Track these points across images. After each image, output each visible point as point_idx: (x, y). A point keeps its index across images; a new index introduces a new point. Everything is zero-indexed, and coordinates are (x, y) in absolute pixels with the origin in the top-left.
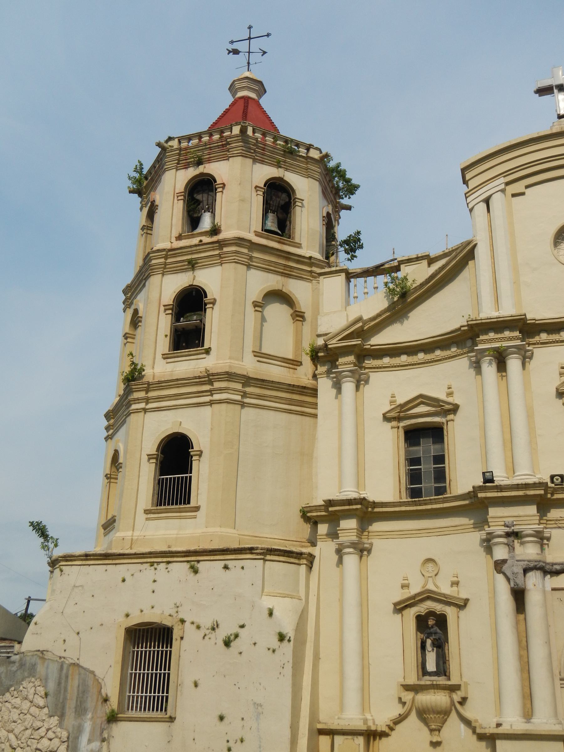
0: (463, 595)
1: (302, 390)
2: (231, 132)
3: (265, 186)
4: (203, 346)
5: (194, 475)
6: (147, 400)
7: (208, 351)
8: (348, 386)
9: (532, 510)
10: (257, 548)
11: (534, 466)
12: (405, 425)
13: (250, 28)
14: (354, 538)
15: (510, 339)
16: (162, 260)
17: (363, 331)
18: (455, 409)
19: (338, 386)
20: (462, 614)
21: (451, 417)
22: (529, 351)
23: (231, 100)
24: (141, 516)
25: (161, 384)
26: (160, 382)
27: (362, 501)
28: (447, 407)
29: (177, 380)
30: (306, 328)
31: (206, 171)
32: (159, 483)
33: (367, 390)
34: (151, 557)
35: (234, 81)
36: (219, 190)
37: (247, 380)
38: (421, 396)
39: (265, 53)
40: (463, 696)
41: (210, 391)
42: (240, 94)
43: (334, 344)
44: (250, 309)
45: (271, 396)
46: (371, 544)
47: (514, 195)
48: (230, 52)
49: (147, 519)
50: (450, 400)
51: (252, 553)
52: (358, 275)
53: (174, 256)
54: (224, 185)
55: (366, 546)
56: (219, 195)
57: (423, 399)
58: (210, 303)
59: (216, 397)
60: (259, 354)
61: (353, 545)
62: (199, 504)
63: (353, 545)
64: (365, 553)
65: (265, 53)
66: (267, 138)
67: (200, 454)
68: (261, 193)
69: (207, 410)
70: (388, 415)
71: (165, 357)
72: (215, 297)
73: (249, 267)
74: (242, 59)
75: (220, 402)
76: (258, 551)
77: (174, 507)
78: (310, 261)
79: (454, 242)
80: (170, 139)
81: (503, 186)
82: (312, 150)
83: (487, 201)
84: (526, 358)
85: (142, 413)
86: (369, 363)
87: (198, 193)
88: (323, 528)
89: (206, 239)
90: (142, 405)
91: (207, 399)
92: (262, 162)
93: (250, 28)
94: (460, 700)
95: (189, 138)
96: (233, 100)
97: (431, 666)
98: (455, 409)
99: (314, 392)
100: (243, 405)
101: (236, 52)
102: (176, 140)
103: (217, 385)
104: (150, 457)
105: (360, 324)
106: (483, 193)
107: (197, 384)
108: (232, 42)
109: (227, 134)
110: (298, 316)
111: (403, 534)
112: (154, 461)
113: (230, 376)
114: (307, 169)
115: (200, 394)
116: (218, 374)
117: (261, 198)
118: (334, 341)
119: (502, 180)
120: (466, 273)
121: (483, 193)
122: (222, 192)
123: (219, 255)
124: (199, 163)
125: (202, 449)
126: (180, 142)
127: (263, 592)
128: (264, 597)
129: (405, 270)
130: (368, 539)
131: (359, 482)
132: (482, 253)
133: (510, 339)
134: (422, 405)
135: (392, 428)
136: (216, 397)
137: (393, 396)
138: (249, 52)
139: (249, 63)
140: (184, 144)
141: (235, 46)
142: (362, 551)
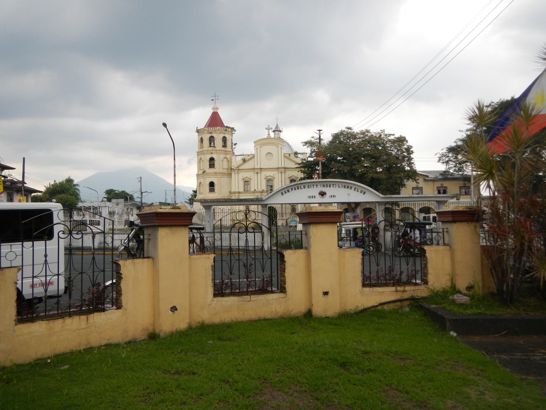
1: (229, 174)
8: (237, 175)
9: (260, 194)
11: (261, 188)
19: (235, 174)
25: (208, 174)
30: (229, 163)
37: (222, 173)
43: (234, 169)
57: (246, 177)
60: (223, 169)
69: (216, 178)
78: (230, 151)
86: (239, 171)
89: (214, 149)
99: (231, 174)
101: (213, 100)
106: (257, 147)
113: (220, 173)
119: (259, 146)
120: (253, 159)
123: (216, 152)
131: (238, 189)
132: (256, 157)
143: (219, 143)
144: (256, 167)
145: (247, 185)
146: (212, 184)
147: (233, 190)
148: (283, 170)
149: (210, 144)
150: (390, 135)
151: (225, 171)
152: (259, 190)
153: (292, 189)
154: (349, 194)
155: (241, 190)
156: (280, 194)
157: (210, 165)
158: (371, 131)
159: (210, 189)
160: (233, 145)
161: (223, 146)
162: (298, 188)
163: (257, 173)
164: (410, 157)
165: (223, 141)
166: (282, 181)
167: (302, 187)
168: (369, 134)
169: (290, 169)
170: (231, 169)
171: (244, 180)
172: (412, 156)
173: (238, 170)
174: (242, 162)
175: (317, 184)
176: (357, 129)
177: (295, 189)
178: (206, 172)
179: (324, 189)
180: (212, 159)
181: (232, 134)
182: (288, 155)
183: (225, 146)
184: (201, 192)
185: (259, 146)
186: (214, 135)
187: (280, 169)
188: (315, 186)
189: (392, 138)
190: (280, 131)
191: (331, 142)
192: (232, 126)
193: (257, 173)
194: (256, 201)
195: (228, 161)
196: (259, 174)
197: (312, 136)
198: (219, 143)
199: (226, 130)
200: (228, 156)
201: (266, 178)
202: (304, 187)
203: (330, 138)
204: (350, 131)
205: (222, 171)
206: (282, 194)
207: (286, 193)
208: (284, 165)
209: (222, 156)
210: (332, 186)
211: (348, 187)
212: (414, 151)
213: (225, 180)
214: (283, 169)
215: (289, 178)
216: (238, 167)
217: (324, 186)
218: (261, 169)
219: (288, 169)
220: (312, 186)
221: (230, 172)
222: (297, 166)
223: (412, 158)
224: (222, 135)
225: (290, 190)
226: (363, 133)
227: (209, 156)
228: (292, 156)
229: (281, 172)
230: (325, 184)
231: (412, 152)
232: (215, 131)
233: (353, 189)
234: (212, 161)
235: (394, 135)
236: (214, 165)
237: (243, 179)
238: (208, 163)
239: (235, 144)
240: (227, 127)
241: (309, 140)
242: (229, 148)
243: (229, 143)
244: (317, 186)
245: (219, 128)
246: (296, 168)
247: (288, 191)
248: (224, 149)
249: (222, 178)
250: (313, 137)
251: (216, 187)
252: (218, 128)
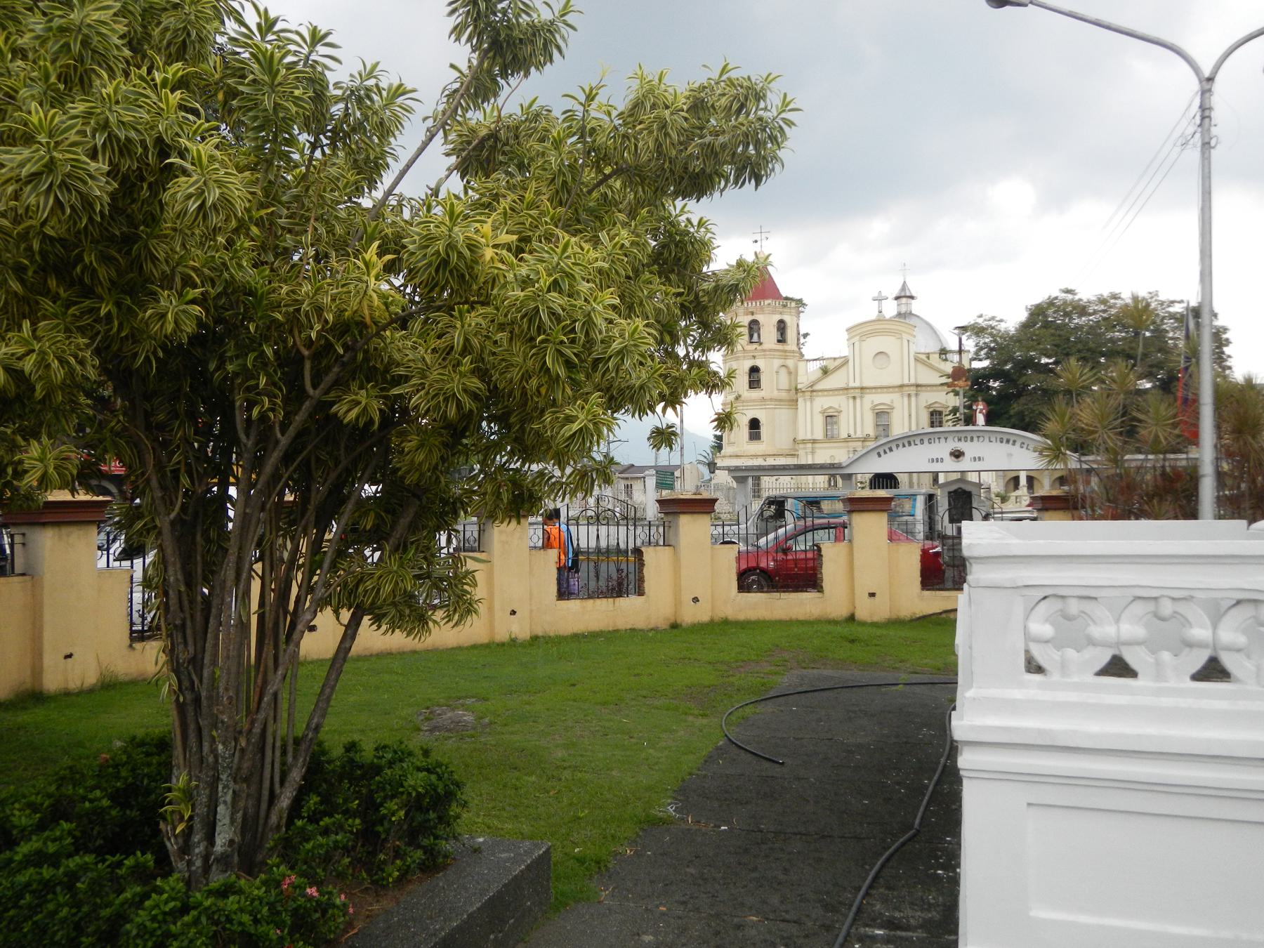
8: (808, 403)
9: (860, 443)
11: (862, 432)
25: (747, 401)
30: (793, 376)
33: (814, 403)
37: (776, 400)
52: (809, 361)
57: (830, 408)
78: (793, 352)
89: (759, 348)
101: (756, 241)
106: (852, 341)
111: (825, 448)
113: (771, 400)
119: (858, 338)
120: (845, 367)
131: (812, 434)
132: (851, 363)
143: (769, 334)
144: (852, 384)
145: (832, 424)
146: (755, 424)
147: (801, 437)
148: (912, 391)
149: (751, 336)
150: (1173, 302)
151: (784, 395)
152: (859, 434)
153: (898, 446)
154: (1010, 455)
155: (819, 434)
156: (875, 454)
157: (750, 382)
158: (1122, 296)
159: (750, 433)
160: (802, 338)
161: (779, 341)
162: (910, 444)
163: (854, 398)
164: (1223, 353)
165: (778, 330)
166: (910, 415)
167: (918, 442)
168: (1119, 302)
170: (797, 390)
172: (1226, 349)
173: (812, 391)
174: (820, 373)
175: (946, 435)
176: (1087, 293)
177: (904, 446)
178: (742, 398)
179: (961, 446)
180: (754, 370)
181: (800, 312)
182: (924, 357)
183: (782, 340)
184: (732, 440)
185: (858, 338)
186: (758, 317)
188: (943, 440)
189: (1177, 308)
190: (912, 297)
191: (1025, 326)
192: (798, 297)
193: (854, 398)
194: (830, 468)
195: (790, 373)
196: (858, 401)
197: (979, 314)
198: (769, 334)
199: (785, 306)
200: (790, 363)
201: (873, 409)
202: (922, 441)
203: (1023, 316)
204: (1070, 297)
205: (776, 394)
206: (879, 455)
207: (885, 452)
208: (916, 378)
209: (777, 363)
210: (975, 439)
211: (1008, 441)
212: (1232, 340)
213: (783, 414)
215: (928, 407)
216: (811, 386)
217: (960, 440)
218: (862, 388)
220: (937, 440)
221: (794, 395)
222: (944, 380)
223: (1229, 356)
224: (778, 317)
225: (894, 448)
226: (1103, 301)
227: (748, 364)
228: (935, 359)
229: (909, 396)
230: (963, 435)
231: (1228, 342)
232: (762, 308)
233: (1018, 444)
234: (755, 375)
235: (1181, 302)
236: (759, 381)
237: (823, 412)
238: (746, 379)
239: (805, 335)
240: (787, 298)
241: (972, 322)
242: (791, 345)
243: (791, 334)
244: (946, 439)
245: (770, 301)
246: (942, 384)
247: (891, 450)
248: (780, 347)
250: (981, 316)
251: (764, 430)
252: (767, 302)
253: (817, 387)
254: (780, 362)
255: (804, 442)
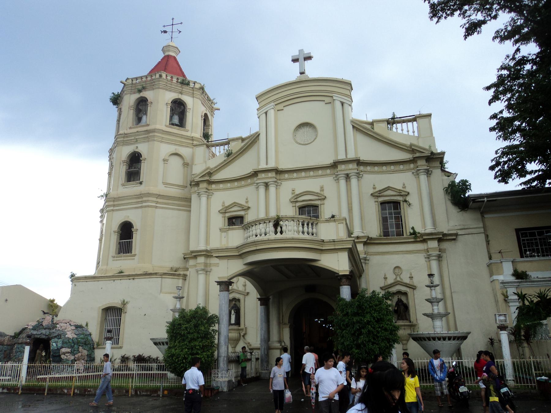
0: (247, 291)
2: (156, 76)
3: (171, 103)
4: (139, 180)
5: (134, 240)
6: (114, 206)
7: (141, 183)
8: (204, 199)
10: (158, 273)
12: (228, 216)
13: (173, 19)
14: (203, 267)
15: (271, 178)
16: (122, 139)
17: (211, 173)
18: (249, 208)
20: (247, 298)
21: (246, 212)
22: (279, 183)
23: (163, 56)
24: (111, 259)
26: (119, 197)
27: (207, 251)
28: (245, 208)
29: (127, 196)
31: (143, 96)
32: (119, 244)
34: (113, 278)
35: (163, 47)
36: (149, 105)
37: (159, 196)
38: (235, 203)
39: (180, 32)
40: (244, 333)
41: (141, 201)
42: (167, 54)
43: (197, 179)
44: (161, 163)
45: (170, 203)
46: (211, 269)
47: (278, 110)
48: (162, 32)
49: (113, 260)
50: (247, 205)
51: (156, 275)
53: (127, 137)
54: (152, 103)
55: (209, 270)
56: (149, 108)
57: (235, 204)
58: (143, 160)
59: (144, 204)
61: (203, 270)
62: (136, 253)
63: (203, 270)
64: (208, 273)
65: (180, 32)
66: (173, 79)
67: (137, 230)
68: (170, 107)
70: (220, 211)
71: (123, 185)
72: (146, 157)
73: (162, 142)
74: (168, 35)
75: (146, 207)
76: (159, 274)
77: (128, 254)
79: (253, 132)
80: (128, 79)
81: (273, 107)
82: (196, 84)
83: (266, 113)
84: (277, 186)
85: (111, 213)
86: (214, 186)
87: (141, 105)
88: (192, 262)
90: (112, 208)
91: (140, 205)
92: (170, 91)
93: (173, 19)
94: (243, 335)
95: (137, 79)
96: (164, 56)
97: (233, 321)
98: (249, 208)
100: (156, 207)
101: (165, 32)
102: (131, 80)
103: (145, 199)
104: (115, 232)
105: (209, 170)
106: (264, 110)
107: (136, 198)
108: (164, 26)
109: (154, 77)
110: (185, 165)
112: (117, 234)
113: (149, 195)
114: (193, 93)
115: (138, 203)
116: (144, 194)
117: (169, 109)
118: (197, 178)
119: (273, 104)
121: (264, 110)
122: (150, 106)
123: (148, 137)
124: (140, 91)
125: (137, 228)
126: (132, 81)
127: (161, 291)
128: (161, 294)
129: (232, 144)
130: (210, 267)
132: (262, 138)
133: (271, 178)
134: (235, 207)
135: (223, 217)
136: (144, 204)
137: (224, 203)
138: (172, 32)
139: (172, 37)
140: (134, 82)
141: (165, 29)
142: (207, 272)
165: (173, 112)
169: (376, 168)
171: (228, 215)
173: (210, 183)
187: (343, 167)
193: (267, 185)
195: (186, 165)
196: (272, 189)
200: (185, 151)
205: (161, 189)
214: (351, 166)
216: (210, 174)
219: (369, 168)
249: (158, 211)
251: (137, 240)
253: (218, 176)
254: (172, 149)
255: (195, 255)
